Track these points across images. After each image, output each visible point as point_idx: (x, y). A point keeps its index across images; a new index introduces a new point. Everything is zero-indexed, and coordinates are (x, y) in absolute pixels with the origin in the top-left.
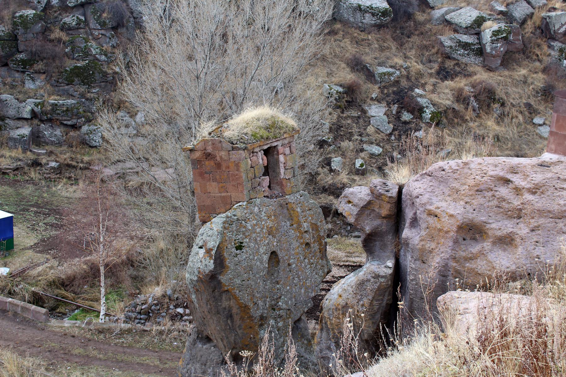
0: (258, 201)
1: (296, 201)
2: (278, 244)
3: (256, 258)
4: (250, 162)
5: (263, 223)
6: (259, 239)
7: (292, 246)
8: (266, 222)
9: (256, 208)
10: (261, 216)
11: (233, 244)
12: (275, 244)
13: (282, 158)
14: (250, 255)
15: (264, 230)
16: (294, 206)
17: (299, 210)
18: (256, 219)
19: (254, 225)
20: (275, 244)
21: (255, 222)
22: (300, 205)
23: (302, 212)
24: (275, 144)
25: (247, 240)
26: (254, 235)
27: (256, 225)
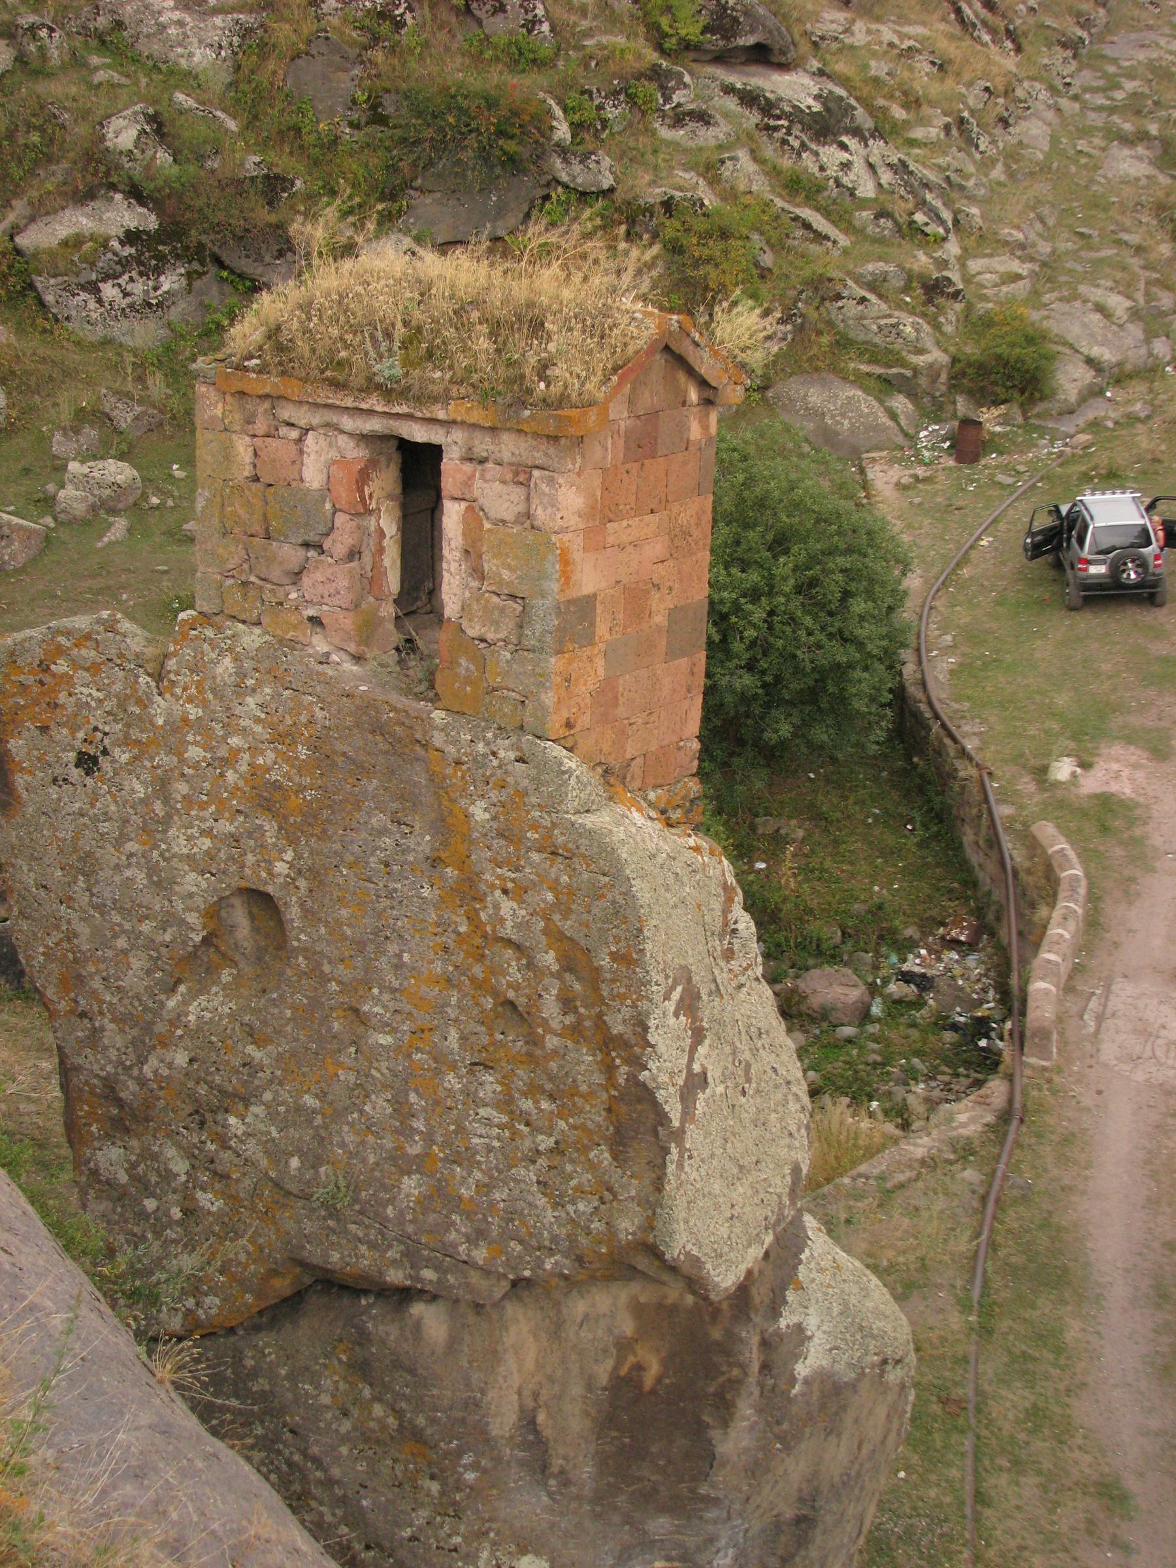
0: (252, 638)
1: (479, 762)
2: (302, 883)
3: (132, 846)
4: (243, 448)
5: (235, 741)
6: (182, 788)
7: (393, 948)
8: (253, 750)
9: (227, 661)
10: (238, 710)
11: (81, 735)
12: (281, 867)
13: (452, 516)
14: (107, 818)
15: (231, 776)
16: (455, 777)
17: (479, 812)
18: (205, 704)
19: (185, 720)
20: (281, 867)
21: (194, 712)
22: (494, 795)
23: (501, 835)
24: (419, 434)
25: (125, 758)
26: (163, 759)
27: (199, 726)
